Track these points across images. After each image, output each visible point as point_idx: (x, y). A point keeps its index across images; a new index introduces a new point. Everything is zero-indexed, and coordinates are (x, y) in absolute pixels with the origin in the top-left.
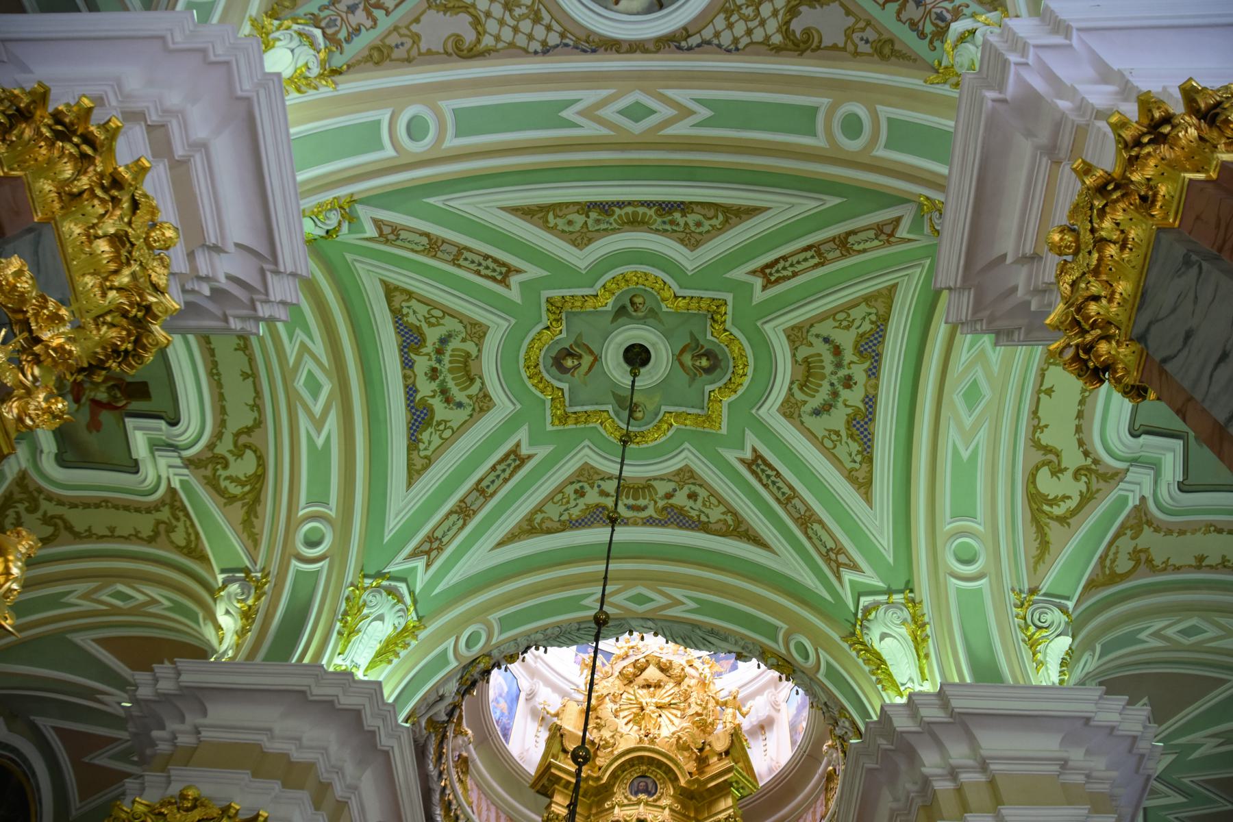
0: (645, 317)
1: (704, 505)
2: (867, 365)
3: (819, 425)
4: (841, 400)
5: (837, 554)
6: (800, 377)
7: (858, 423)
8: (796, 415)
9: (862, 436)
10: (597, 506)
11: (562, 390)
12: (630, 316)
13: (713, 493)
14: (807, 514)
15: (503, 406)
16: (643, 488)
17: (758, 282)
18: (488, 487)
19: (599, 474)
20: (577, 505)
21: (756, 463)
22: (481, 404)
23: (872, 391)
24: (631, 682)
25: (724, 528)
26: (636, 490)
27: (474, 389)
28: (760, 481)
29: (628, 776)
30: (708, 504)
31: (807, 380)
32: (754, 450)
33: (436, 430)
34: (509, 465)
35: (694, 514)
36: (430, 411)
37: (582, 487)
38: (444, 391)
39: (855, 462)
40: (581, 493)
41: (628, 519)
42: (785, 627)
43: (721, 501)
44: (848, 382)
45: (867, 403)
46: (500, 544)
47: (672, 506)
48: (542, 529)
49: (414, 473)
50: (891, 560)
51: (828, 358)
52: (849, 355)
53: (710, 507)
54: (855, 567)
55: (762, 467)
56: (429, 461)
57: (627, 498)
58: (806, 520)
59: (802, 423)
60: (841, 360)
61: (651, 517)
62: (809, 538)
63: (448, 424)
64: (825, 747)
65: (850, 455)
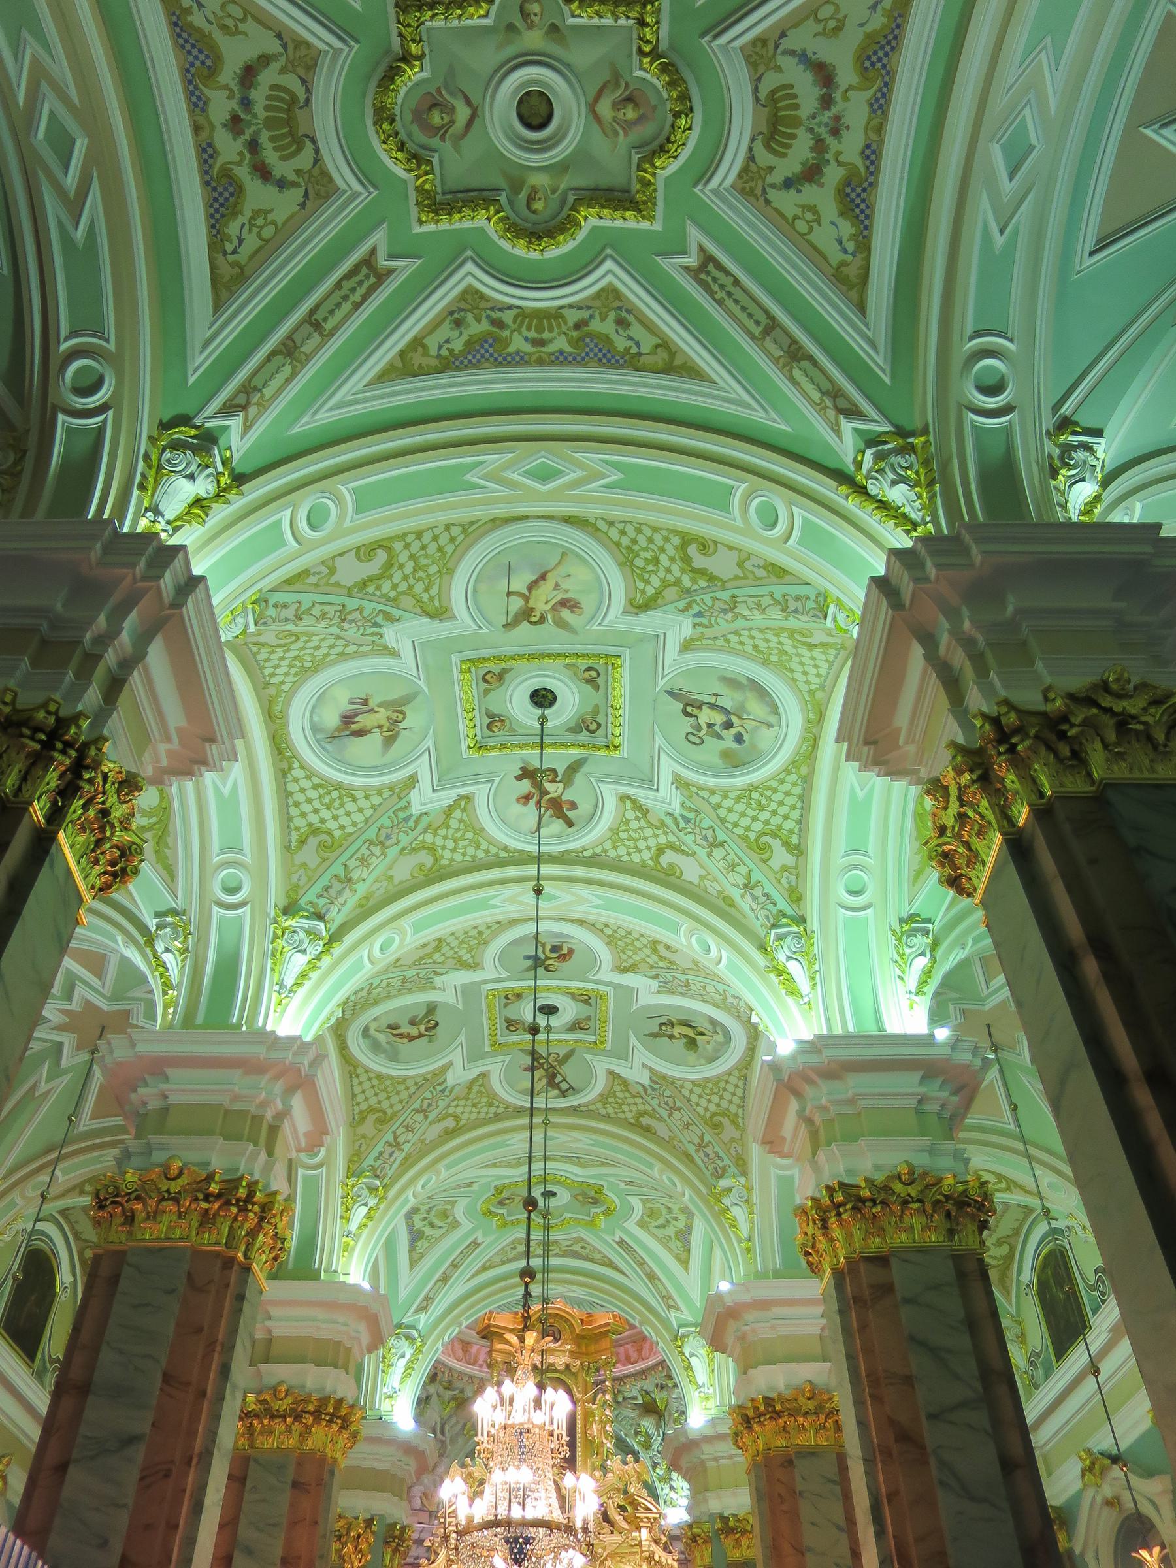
3: (660, 1232)
13: (595, 1248)
15: (466, 1225)
17: (622, 1185)
21: (621, 1243)
27: (449, 1221)
36: (423, 1232)
38: (432, 1225)
43: (600, 1252)
49: (413, 1263)
51: (664, 1211)
54: (678, 1309)
56: (422, 1255)
58: (652, 1277)
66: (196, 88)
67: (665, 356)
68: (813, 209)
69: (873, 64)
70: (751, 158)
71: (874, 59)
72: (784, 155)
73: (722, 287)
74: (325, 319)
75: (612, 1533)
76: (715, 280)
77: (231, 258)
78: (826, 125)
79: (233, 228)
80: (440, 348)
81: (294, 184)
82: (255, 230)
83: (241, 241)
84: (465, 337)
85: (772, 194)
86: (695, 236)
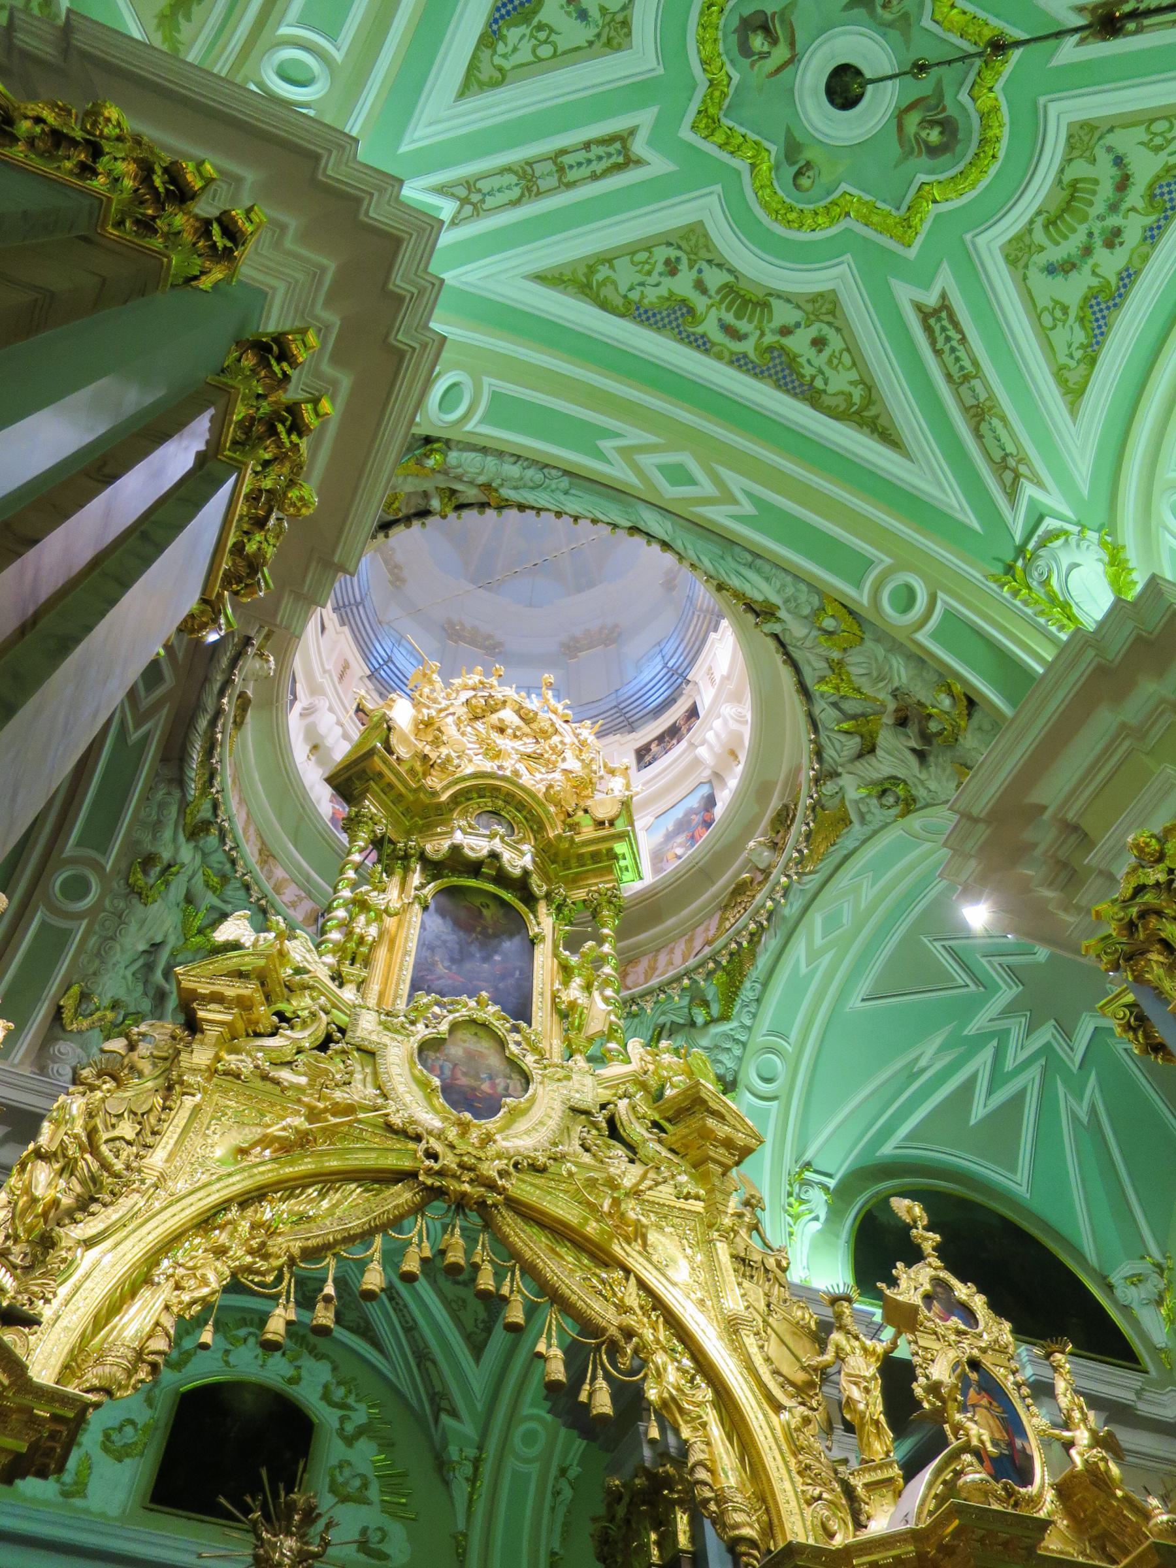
0: (890, 25)
1: (830, 362)
2: (1150, 220)
4: (1091, 262)
5: (1020, 461)
6: (1053, 210)
7: (1098, 304)
8: (1021, 264)
9: (1095, 324)
10: (684, 301)
11: (730, 78)
12: (872, 12)
14: (988, 403)
16: (758, 303)
18: (571, 167)
19: (709, 251)
20: (657, 285)
22: (613, 34)
23: (1136, 263)
24: (477, 718)
25: (843, 407)
26: (746, 302)
28: (933, 343)
29: (475, 806)
30: (835, 361)
31: (1060, 217)
32: (944, 296)
33: (532, 36)
34: (609, 155)
35: (808, 371)
37: (678, 259)
39: (1071, 356)
40: (672, 268)
41: (713, 344)
42: (888, 561)
44: (1113, 238)
45: (1122, 279)
46: (540, 278)
47: (782, 348)
48: (598, 295)
50: (1085, 491)
51: (1106, 190)
52: (1135, 196)
53: (836, 368)
55: (945, 323)
56: (501, 79)
57: (728, 309)
59: (1025, 278)
60: (1121, 200)
61: (745, 356)
62: (979, 436)
63: (553, 37)
64: (752, 844)
65: (1070, 346)
75: (632, 1161)
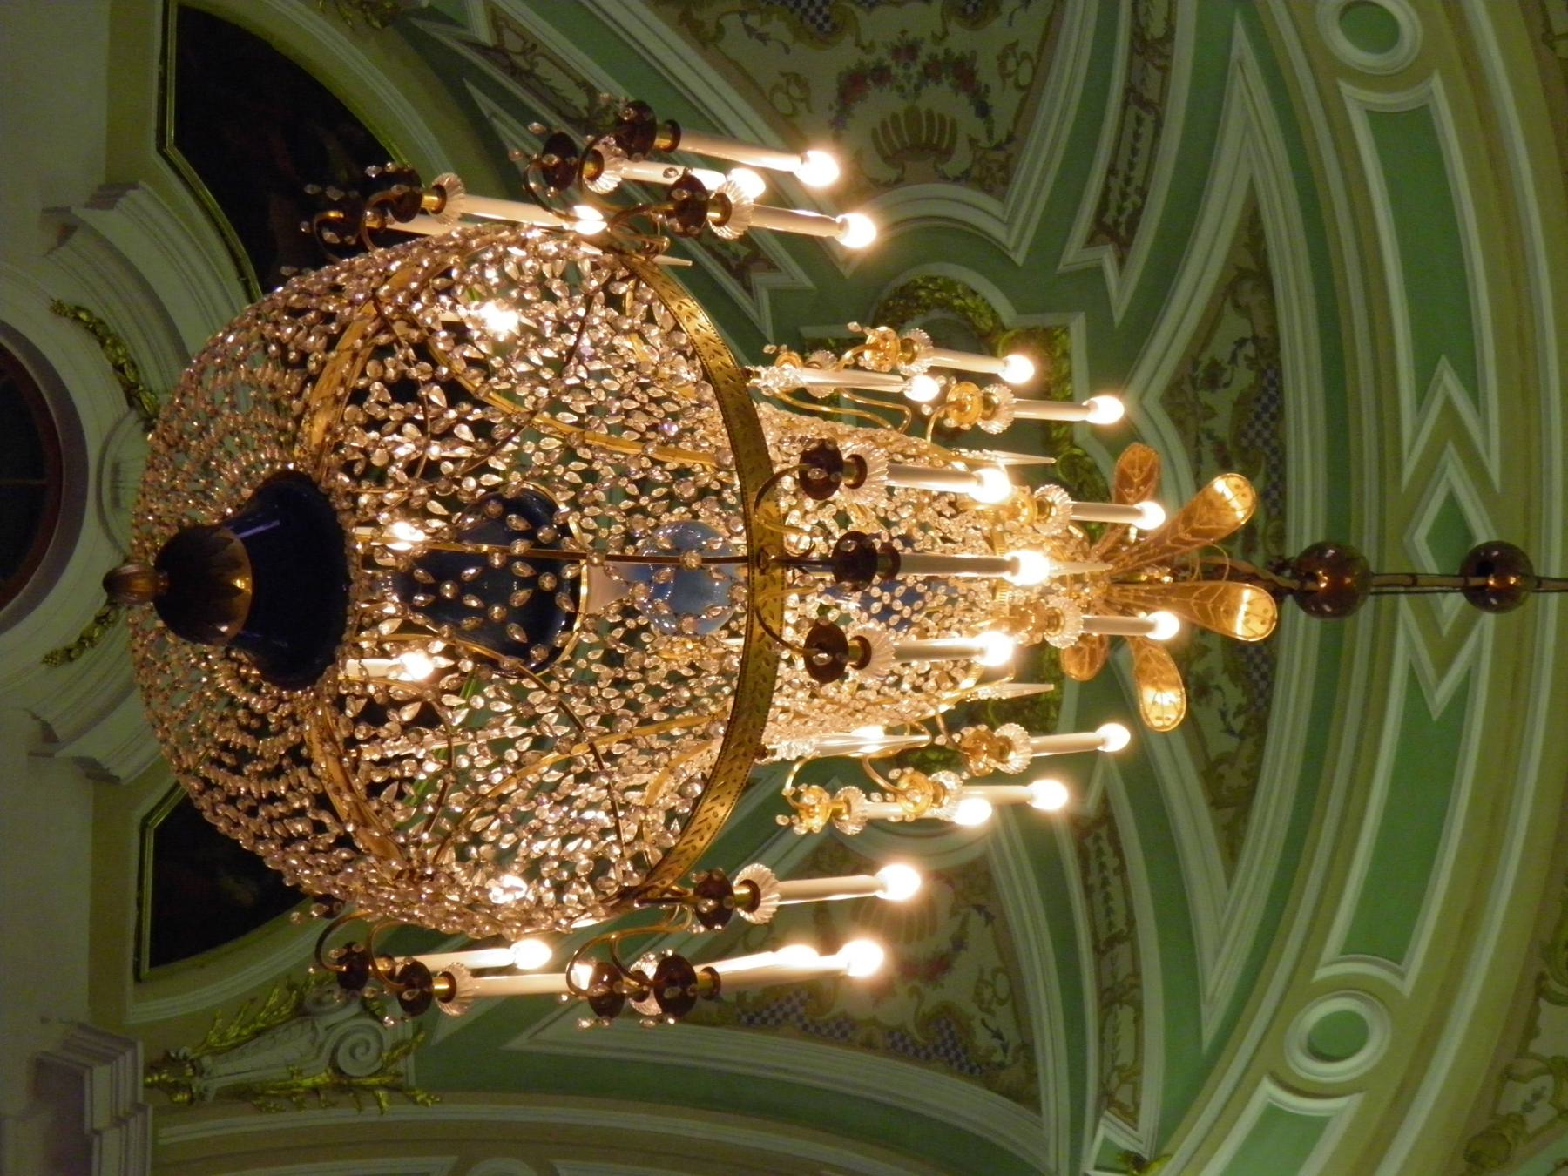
66: (826, 1025)
67: (1247, 286)
68: (1002, 60)
69: (827, 19)
70: (963, 178)
71: (820, 20)
72: (953, 124)
73: (1124, 196)
74: (1111, 925)
76: (1120, 210)
77: (1009, 1060)
78: (907, 66)
79: (983, 1039)
80: (1230, 731)
81: (964, 924)
82: (994, 1006)
83: (997, 1035)
84: (1223, 680)
85: (1000, 134)
86: (1074, 254)
